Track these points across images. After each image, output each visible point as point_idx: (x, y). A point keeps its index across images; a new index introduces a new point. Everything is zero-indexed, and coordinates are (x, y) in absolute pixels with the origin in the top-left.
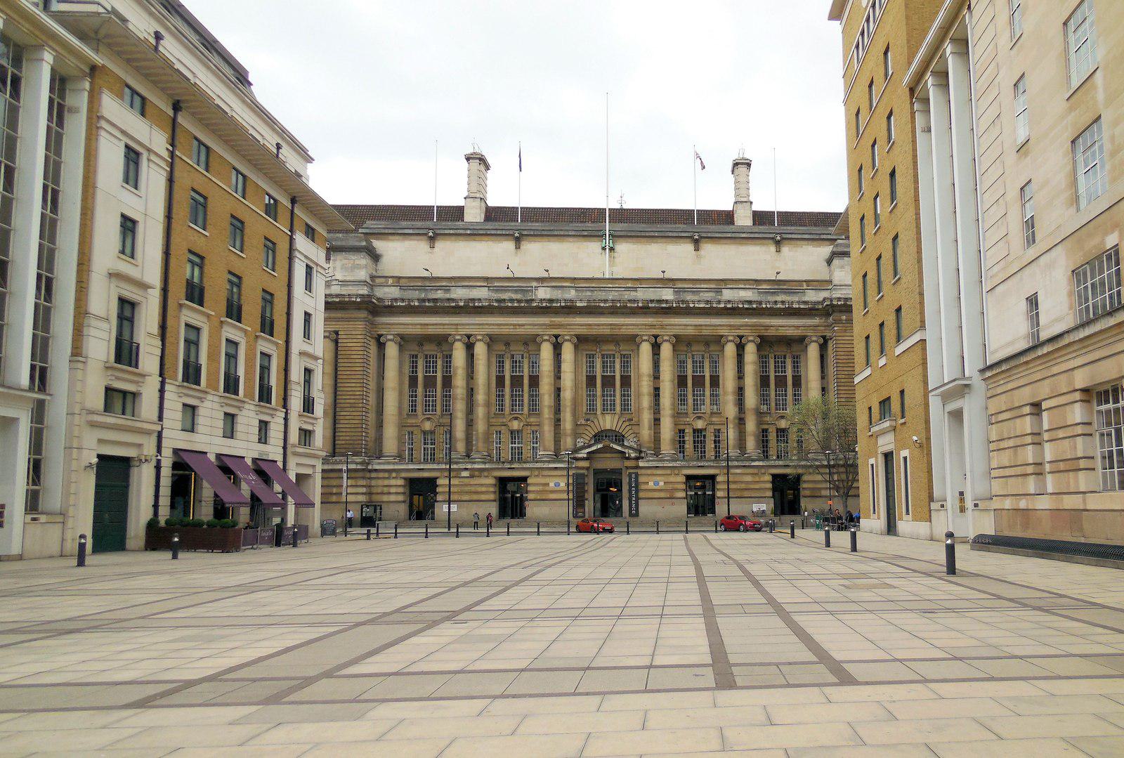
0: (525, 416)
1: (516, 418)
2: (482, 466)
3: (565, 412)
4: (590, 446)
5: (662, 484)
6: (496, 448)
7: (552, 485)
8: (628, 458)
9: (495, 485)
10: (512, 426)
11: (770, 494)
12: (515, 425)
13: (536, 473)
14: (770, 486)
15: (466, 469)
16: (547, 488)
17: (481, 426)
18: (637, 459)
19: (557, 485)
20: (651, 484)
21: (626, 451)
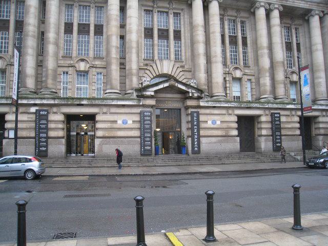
0: (91, 59)
1: (82, 60)
2: (52, 102)
3: (131, 53)
4: (157, 84)
5: (218, 122)
6: (63, 88)
7: (120, 122)
8: (191, 98)
9: (63, 122)
10: (79, 67)
11: (298, 132)
12: (82, 66)
13: (105, 110)
14: (298, 125)
15: (35, 105)
16: (115, 126)
17: (51, 63)
18: (199, 98)
19: (125, 122)
20: (210, 122)
21: (190, 90)
